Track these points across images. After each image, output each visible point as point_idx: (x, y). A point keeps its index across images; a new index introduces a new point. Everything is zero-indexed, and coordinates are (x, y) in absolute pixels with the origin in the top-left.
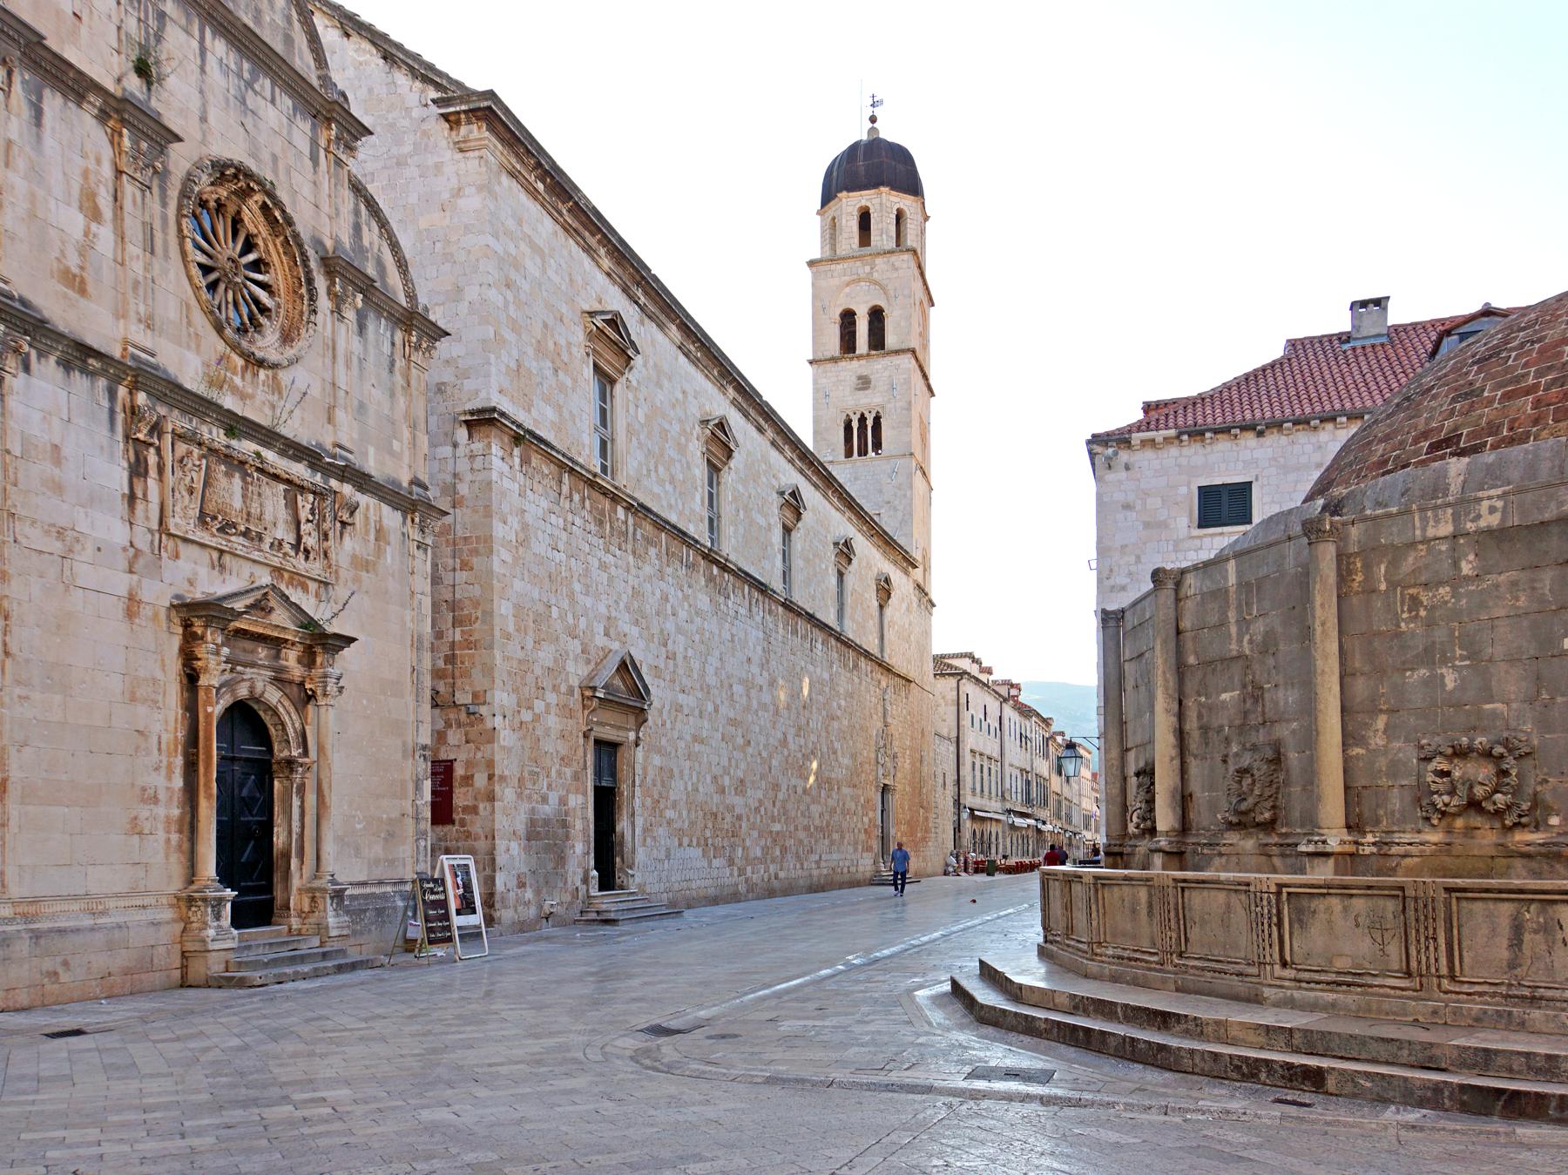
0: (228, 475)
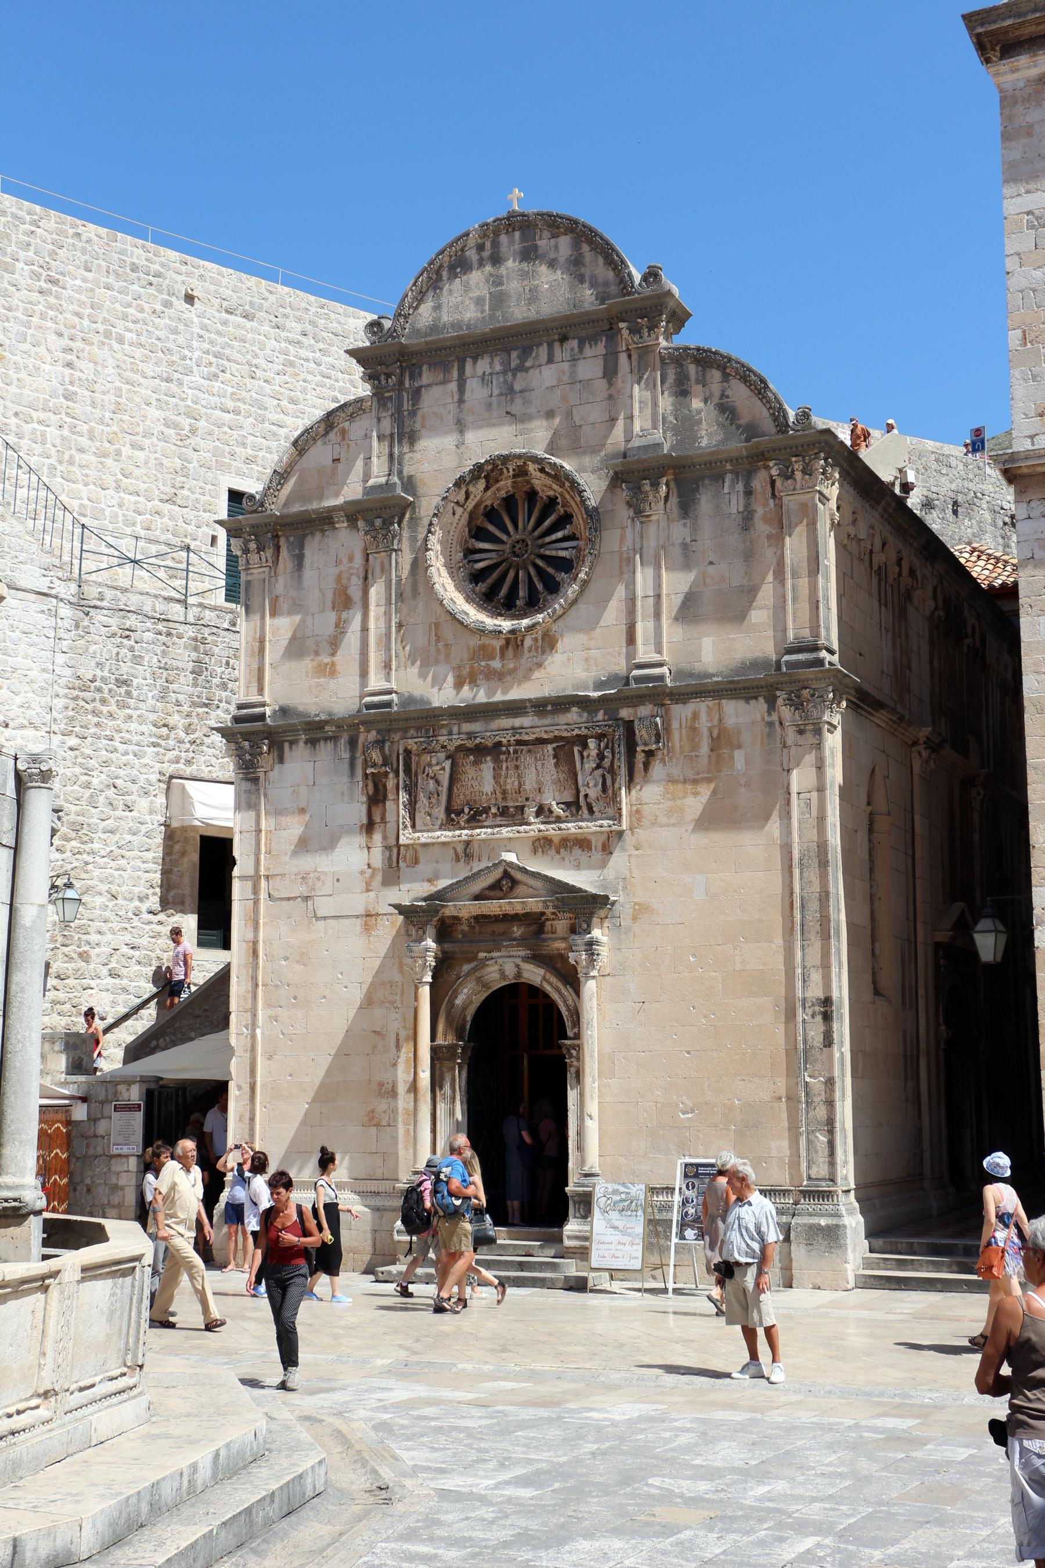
0: (476, 763)
